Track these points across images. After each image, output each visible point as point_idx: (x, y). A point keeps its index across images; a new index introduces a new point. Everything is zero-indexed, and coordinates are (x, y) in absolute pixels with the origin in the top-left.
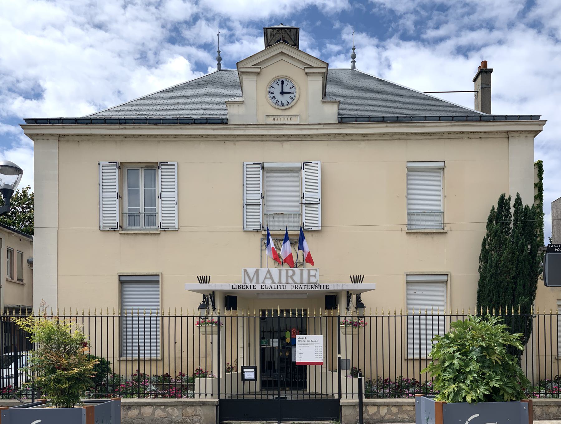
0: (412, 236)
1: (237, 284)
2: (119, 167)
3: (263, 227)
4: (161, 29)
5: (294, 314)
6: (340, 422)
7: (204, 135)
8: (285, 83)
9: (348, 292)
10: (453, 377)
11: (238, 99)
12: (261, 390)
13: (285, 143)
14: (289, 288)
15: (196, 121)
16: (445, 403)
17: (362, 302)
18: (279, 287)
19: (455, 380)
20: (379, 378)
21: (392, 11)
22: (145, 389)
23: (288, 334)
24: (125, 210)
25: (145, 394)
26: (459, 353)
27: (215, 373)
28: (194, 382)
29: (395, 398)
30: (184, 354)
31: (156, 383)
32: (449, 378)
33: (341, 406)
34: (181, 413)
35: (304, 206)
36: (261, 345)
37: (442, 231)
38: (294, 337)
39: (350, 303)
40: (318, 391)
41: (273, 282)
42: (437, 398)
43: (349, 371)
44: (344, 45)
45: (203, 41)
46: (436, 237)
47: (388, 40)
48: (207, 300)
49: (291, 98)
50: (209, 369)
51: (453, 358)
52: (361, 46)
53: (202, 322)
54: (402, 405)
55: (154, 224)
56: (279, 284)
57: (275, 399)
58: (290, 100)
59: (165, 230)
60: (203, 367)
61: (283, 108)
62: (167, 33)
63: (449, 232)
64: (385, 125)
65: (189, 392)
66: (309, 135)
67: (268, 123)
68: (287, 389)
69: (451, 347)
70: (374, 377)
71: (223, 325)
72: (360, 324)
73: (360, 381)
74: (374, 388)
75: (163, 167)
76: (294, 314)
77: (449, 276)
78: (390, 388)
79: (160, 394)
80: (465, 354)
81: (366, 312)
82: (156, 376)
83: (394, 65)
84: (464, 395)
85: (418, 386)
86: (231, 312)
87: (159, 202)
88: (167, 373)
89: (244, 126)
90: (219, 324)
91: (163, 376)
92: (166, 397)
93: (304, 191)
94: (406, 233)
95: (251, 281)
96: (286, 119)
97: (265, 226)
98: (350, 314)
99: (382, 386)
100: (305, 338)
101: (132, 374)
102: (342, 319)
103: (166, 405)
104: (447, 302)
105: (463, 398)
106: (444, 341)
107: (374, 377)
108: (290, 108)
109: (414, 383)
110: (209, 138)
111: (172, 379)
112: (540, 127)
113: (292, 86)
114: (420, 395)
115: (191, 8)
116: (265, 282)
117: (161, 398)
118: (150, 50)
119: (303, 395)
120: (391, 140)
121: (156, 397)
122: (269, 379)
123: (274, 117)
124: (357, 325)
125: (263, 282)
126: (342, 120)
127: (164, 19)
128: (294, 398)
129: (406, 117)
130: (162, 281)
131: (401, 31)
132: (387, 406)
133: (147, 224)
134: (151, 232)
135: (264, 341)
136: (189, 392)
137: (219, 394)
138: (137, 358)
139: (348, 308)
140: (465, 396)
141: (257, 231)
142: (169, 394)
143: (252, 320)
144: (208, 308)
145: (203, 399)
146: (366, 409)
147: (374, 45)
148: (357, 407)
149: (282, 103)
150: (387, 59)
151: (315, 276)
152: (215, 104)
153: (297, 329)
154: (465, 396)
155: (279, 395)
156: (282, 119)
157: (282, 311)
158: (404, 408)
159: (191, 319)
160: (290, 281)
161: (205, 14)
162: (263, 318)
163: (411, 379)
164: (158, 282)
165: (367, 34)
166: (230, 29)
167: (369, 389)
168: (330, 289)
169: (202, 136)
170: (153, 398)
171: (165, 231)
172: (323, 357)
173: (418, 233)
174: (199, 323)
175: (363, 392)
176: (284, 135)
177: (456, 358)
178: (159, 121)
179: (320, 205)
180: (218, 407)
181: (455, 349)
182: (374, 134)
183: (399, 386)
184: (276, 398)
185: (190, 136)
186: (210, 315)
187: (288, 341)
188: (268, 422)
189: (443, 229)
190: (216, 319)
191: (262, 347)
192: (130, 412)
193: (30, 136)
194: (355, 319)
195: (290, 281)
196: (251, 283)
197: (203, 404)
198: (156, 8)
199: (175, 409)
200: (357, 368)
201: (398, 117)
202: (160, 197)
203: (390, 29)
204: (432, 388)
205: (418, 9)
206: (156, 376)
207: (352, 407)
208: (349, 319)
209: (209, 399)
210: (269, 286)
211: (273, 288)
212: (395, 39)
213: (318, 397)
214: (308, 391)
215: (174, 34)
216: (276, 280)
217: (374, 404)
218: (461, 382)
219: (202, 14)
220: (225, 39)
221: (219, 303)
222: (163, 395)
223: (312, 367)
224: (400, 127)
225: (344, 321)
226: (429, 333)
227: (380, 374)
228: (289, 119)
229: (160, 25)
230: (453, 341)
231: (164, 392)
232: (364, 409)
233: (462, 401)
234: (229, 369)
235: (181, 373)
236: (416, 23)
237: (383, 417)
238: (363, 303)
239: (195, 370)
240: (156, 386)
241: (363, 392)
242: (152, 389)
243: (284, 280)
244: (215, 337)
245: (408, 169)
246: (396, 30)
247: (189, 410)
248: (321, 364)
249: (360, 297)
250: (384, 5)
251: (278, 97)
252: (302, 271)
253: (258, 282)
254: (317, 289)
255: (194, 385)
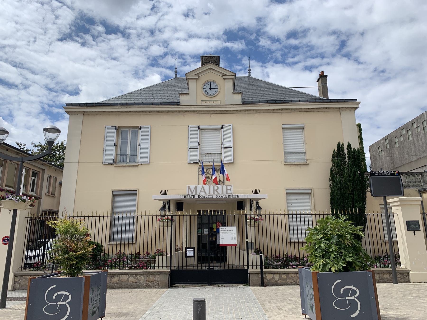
0: (288, 166)
1: (184, 195)
2: (117, 129)
3: (200, 161)
4: (147, 60)
5: (218, 212)
6: (249, 285)
7: (167, 111)
8: (212, 83)
9: (251, 200)
10: (322, 255)
11: (186, 92)
12: (197, 263)
13: (212, 115)
14: (215, 197)
15: (162, 104)
16: (318, 273)
17: (259, 206)
18: (209, 197)
19: (323, 257)
20: (272, 255)
21: (269, 50)
22: (124, 263)
23: (214, 226)
24: (119, 153)
25: (123, 266)
26: (324, 239)
27: (169, 252)
28: (155, 258)
29: (284, 268)
30: (150, 240)
31: (131, 259)
32: (319, 255)
33: (249, 274)
34: (146, 280)
35: (223, 149)
36: (198, 233)
37: (306, 163)
38: (218, 228)
39: (252, 206)
40: (234, 263)
41: (206, 194)
42: (312, 268)
43: (253, 250)
44: (244, 66)
45: (169, 65)
46: (302, 167)
47: (267, 63)
48: (165, 205)
49: (215, 91)
50: (165, 250)
51: (321, 242)
52: (253, 67)
53: (162, 219)
54: (289, 274)
55: (135, 160)
56: (209, 195)
57: (206, 269)
58: (215, 93)
59: (141, 164)
60: (161, 248)
61: (211, 96)
62: (150, 62)
63: (310, 163)
64: (269, 105)
65: (152, 265)
66: (225, 111)
67: (202, 104)
68: (214, 262)
69: (319, 235)
70: (270, 254)
71: (174, 220)
72: (259, 220)
73: (261, 257)
74: (270, 261)
75: (142, 128)
76: (218, 212)
77: (312, 189)
78: (280, 262)
79: (133, 266)
80: (327, 240)
81: (263, 212)
82: (131, 254)
83: (271, 76)
84: (330, 267)
85: (298, 260)
86: (180, 212)
87: (139, 148)
88: (138, 253)
89: (189, 106)
90: (172, 220)
91: (135, 254)
92: (137, 269)
93: (223, 141)
94: (284, 164)
95: (192, 193)
96: (213, 102)
97: (201, 161)
98: (253, 213)
99: (275, 260)
100: (225, 229)
101: (116, 253)
102: (248, 217)
103: (137, 274)
104: (312, 206)
105: (329, 269)
106: (314, 231)
107: (270, 254)
108: (215, 96)
109: (295, 259)
110: (169, 113)
111: (141, 256)
112: (358, 105)
113: (216, 85)
114: (302, 267)
115: (164, 49)
116: (201, 193)
117: (133, 269)
118: (140, 70)
119: (225, 267)
120: (272, 112)
121: (130, 268)
122: (203, 255)
123: (206, 101)
124: (258, 220)
125: (200, 194)
126: (244, 102)
127: (149, 55)
128: (219, 268)
129: (280, 100)
130: (138, 194)
131: (274, 59)
132: (279, 274)
133: (131, 160)
134: (133, 165)
135: (200, 230)
136: (152, 265)
137: (171, 266)
138: (120, 243)
139: (251, 209)
140: (331, 268)
141: (196, 164)
142: (139, 267)
143: (192, 217)
144: (166, 210)
145: (160, 270)
146: (266, 276)
147: (260, 66)
148: (259, 275)
149: (211, 94)
150: (267, 73)
151: (230, 190)
152: (173, 95)
153: (220, 222)
154: (331, 268)
155: (209, 266)
156: (210, 102)
157: (211, 211)
158: (290, 275)
159: (154, 217)
160: (216, 193)
161: (171, 52)
162: (199, 216)
163: (293, 255)
164: (136, 194)
165: (256, 61)
166: (184, 59)
167: (266, 262)
168: (240, 198)
169: (165, 111)
170: (128, 269)
171: (141, 164)
172: (236, 240)
173: (291, 164)
174: (160, 220)
175: (263, 265)
176: (212, 111)
177: (323, 242)
178: (141, 104)
179: (232, 148)
180: (170, 275)
181: (322, 237)
182: (262, 110)
183: (285, 261)
184: (207, 268)
185: (159, 111)
186: (167, 215)
187: (215, 230)
188: (202, 285)
189: (306, 162)
190: (170, 217)
191: (199, 234)
192: (113, 279)
193: (68, 113)
194: (256, 217)
195: (216, 193)
196: (192, 194)
197: (160, 273)
198: (145, 50)
199: (142, 276)
200: (258, 249)
201: (276, 101)
202: (139, 145)
203: (268, 58)
204: (307, 262)
205: (283, 48)
206: (131, 254)
207: (257, 274)
208: (252, 216)
209: (164, 270)
210: (203, 196)
211: (205, 197)
212: (271, 63)
213: (234, 268)
214: (228, 263)
215: (153, 62)
216: (207, 192)
217: (270, 273)
218: (327, 258)
219: (170, 52)
220: (182, 64)
221: (172, 207)
222: (135, 267)
223: (230, 247)
224: (277, 106)
225: (249, 218)
226: (303, 225)
227: (273, 252)
228: (214, 102)
229: (147, 58)
230: (320, 231)
231: (136, 265)
232: (264, 276)
233: (328, 271)
234: (178, 249)
235: (147, 252)
236: (282, 55)
237: (277, 282)
238: (260, 207)
239: (156, 250)
240: (131, 261)
241: (263, 265)
242: (128, 263)
243: (212, 192)
244: (169, 228)
245: (283, 128)
246: (271, 59)
247: (151, 278)
248: (235, 245)
249: (258, 203)
250: (265, 46)
251: (209, 91)
252: (222, 186)
253: (196, 194)
254: (232, 198)
255: (155, 260)
